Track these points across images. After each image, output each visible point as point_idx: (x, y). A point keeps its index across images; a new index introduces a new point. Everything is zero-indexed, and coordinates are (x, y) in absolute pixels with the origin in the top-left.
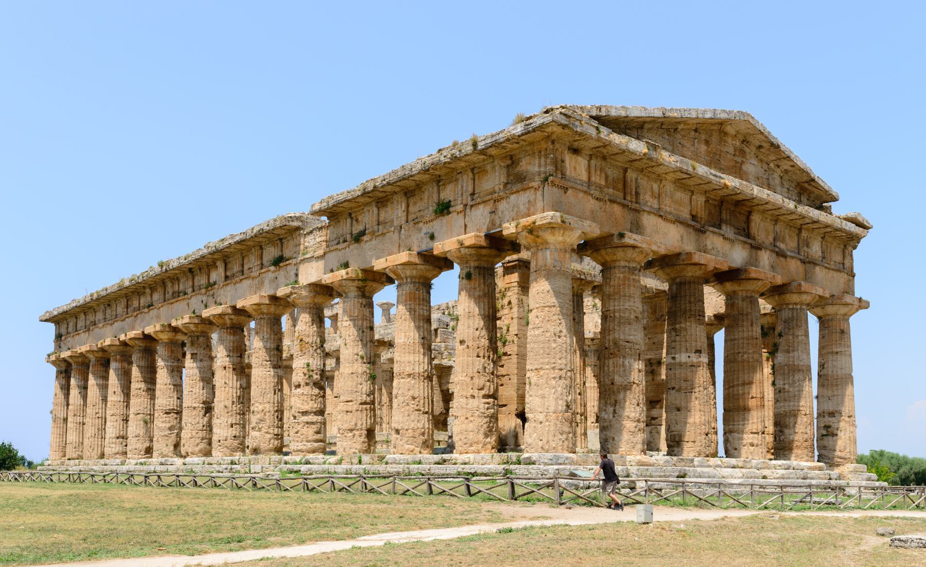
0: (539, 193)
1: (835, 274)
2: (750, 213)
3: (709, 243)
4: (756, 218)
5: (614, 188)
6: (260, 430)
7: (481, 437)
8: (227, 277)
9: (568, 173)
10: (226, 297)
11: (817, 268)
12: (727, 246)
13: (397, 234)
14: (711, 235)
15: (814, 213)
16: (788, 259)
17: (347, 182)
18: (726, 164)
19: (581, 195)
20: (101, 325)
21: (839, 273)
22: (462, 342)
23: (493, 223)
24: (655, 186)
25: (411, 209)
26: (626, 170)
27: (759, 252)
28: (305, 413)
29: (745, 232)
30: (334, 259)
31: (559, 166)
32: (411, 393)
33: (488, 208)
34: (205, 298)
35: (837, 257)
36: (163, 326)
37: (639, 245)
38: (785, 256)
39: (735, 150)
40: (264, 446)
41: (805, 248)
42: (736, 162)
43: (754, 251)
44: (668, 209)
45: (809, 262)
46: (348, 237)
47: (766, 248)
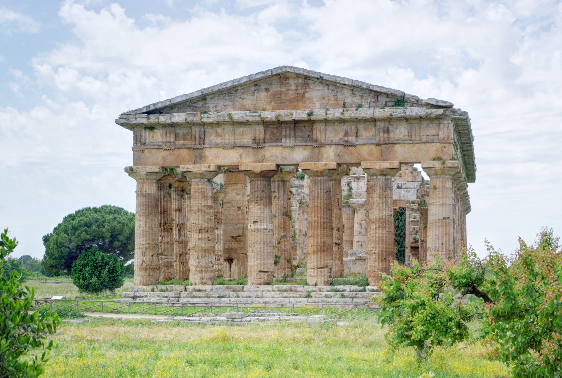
1: (422, 146)
3: (268, 154)
5: (184, 139)
9: (147, 141)
11: (397, 146)
12: (286, 152)
14: (270, 148)
16: (358, 147)
18: (287, 98)
19: (155, 150)
21: (428, 145)
24: (219, 130)
27: (323, 148)
31: (138, 140)
37: (190, 170)
38: (355, 146)
39: (297, 86)
41: (382, 134)
42: (298, 94)
43: (316, 150)
44: (227, 141)
45: (386, 144)
47: (330, 145)
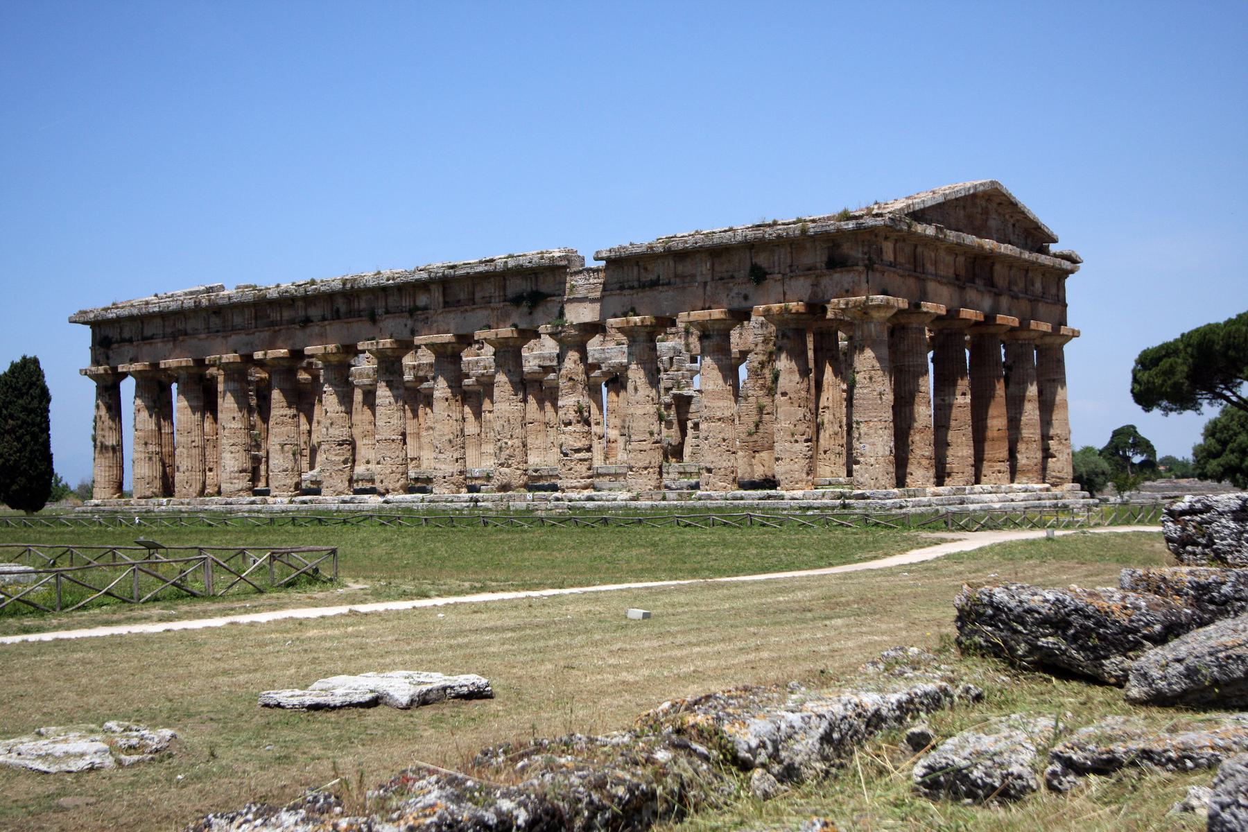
0: (863, 277)
2: (993, 264)
4: (997, 267)
6: (509, 466)
7: (804, 475)
8: (446, 304)
10: (448, 324)
13: (701, 291)
15: (1042, 259)
17: (642, 233)
20: (203, 336)
22: (784, 394)
23: (814, 294)
25: (717, 268)
26: (916, 247)
28: (578, 451)
29: (990, 283)
30: (616, 302)
32: (721, 436)
33: (809, 282)
34: (409, 322)
35: (1053, 291)
36: (337, 348)
40: (514, 482)
46: (636, 284)
